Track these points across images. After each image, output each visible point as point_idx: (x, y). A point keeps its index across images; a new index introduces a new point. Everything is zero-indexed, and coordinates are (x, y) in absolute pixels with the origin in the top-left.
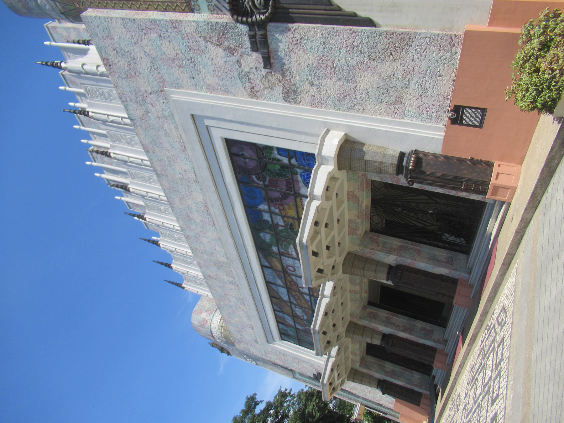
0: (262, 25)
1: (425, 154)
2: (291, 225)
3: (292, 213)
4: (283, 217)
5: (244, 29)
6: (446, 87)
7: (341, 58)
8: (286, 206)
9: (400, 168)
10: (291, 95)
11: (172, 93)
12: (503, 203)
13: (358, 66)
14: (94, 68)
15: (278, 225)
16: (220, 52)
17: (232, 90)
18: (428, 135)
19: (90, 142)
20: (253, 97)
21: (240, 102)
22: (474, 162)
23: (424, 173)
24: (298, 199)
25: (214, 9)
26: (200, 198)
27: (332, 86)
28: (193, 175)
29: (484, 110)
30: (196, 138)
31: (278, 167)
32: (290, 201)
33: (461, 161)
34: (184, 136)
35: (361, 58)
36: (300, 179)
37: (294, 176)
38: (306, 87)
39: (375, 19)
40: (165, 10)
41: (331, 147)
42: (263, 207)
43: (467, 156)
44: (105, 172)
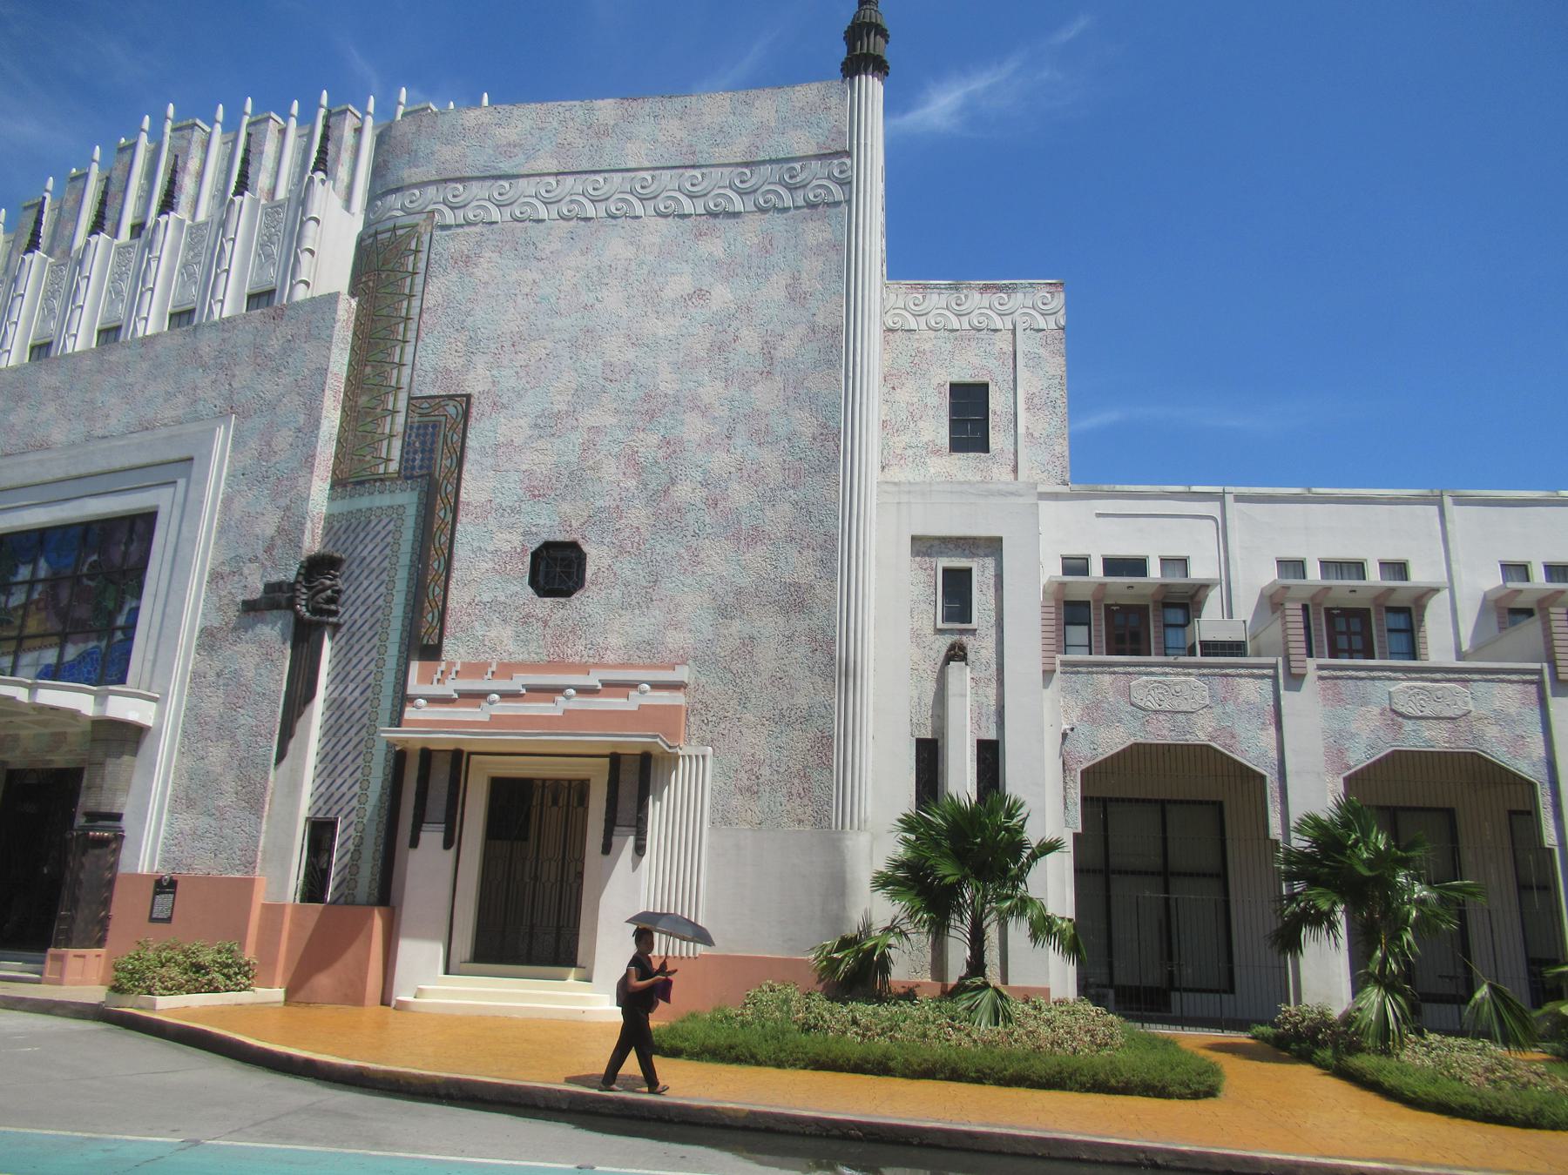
0: (291, 605)
1: (117, 851)
2: (9, 622)
3: (33, 626)
4: (25, 606)
5: (291, 575)
6: (203, 865)
7: (245, 719)
8: (44, 614)
9: (94, 817)
10: (209, 640)
11: (227, 429)
12: (40, 973)
13: (235, 744)
14: (307, 244)
15: (9, 594)
16: (270, 531)
17: (223, 542)
18: (145, 851)
19: (218, 127)
20: (211, 575)
21: (205, 552)
22: (104, 923)
23: (84, 853)
24: (56, 639)
25: (330, 519)
26: (58, 435)
27: (214, 704)
28: (100, 432)
29: (169, 920)
30: (158, 458)
31: (111, 605)
32: (54, 625)
33: (106, 903)
34: (164, 432)
35: (243, 746)
36: (91, 644)
37: (94, 635)
38: (217, 665)
39: (285, 762)
40: (339, 441)
41: (124, 707)
42: (43, 570)
43: (116, 909)
44: (152, 146)
